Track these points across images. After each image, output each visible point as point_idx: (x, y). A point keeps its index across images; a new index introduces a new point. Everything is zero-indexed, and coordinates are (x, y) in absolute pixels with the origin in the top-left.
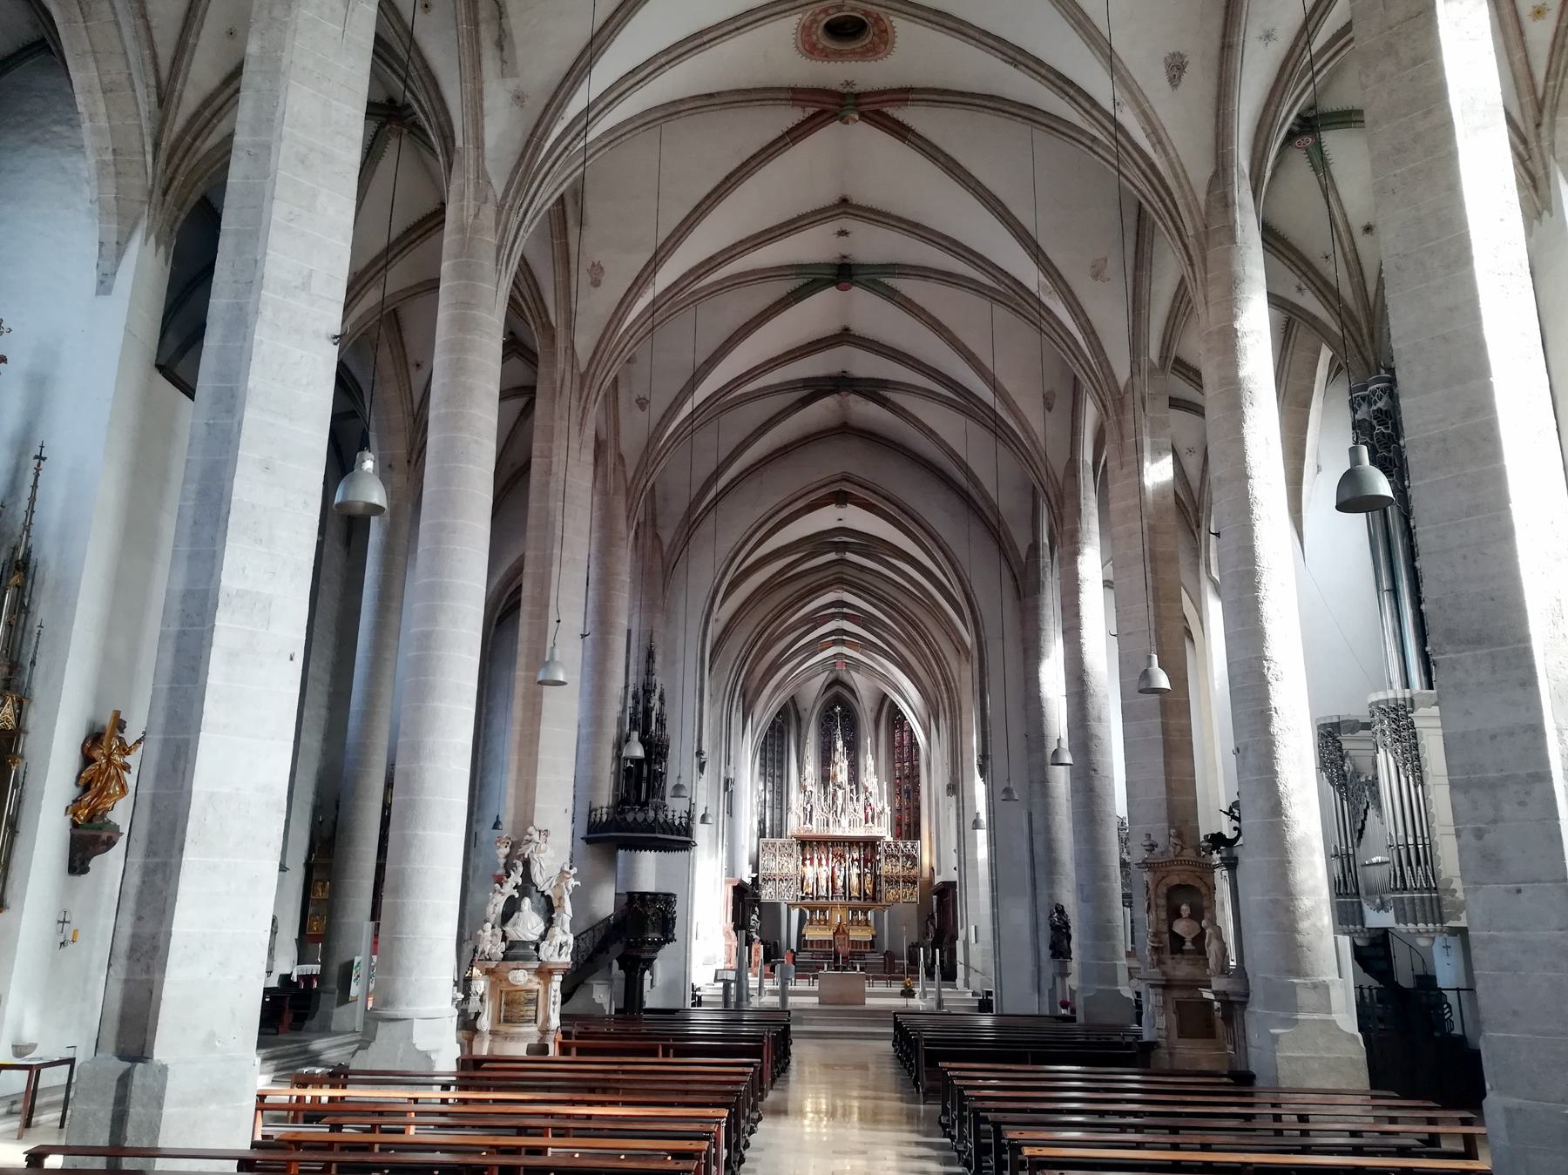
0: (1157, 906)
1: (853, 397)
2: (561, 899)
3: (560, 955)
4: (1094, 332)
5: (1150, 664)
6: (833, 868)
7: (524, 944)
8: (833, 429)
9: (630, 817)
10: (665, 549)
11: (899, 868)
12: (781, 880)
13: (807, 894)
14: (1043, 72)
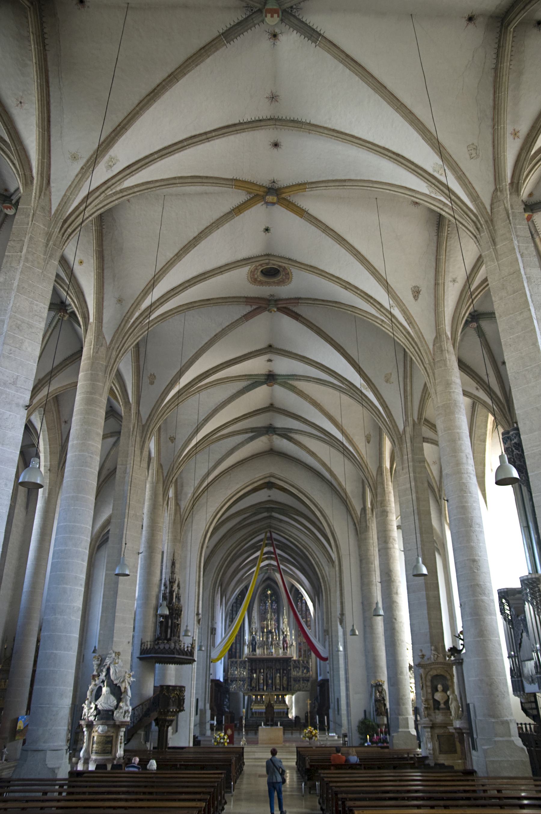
0: (426, 686)
1: (275, 437)
3: (124, 717)
4: (387, 407)
6: (267, 674)
8: (265, 452)
9: (162, 646)
10: (182, 511)
11: (300, 673)
12: (240, 680)
13: (253, 687)
14: (359, 292)
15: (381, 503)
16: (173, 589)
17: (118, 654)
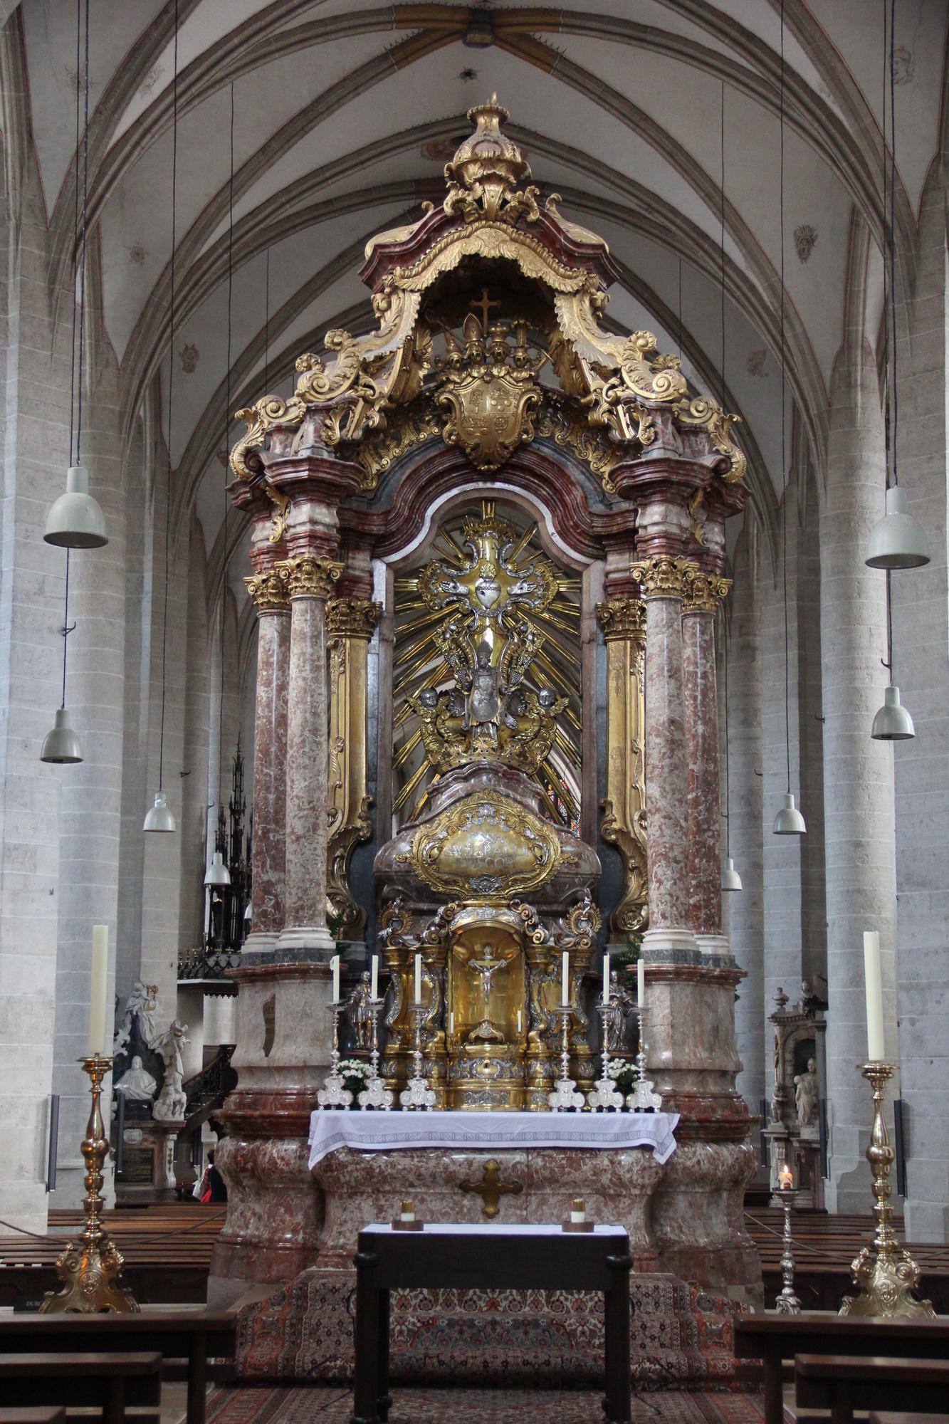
0: (784, 1061)
2: (173, 1057)
3: (173, 1113)
4: (750, 433)
5: (788, 806)
7: (139, 1103)
10: (240, 608)
15: (741, 627)
16: (241, 827)
17: (154, 990)
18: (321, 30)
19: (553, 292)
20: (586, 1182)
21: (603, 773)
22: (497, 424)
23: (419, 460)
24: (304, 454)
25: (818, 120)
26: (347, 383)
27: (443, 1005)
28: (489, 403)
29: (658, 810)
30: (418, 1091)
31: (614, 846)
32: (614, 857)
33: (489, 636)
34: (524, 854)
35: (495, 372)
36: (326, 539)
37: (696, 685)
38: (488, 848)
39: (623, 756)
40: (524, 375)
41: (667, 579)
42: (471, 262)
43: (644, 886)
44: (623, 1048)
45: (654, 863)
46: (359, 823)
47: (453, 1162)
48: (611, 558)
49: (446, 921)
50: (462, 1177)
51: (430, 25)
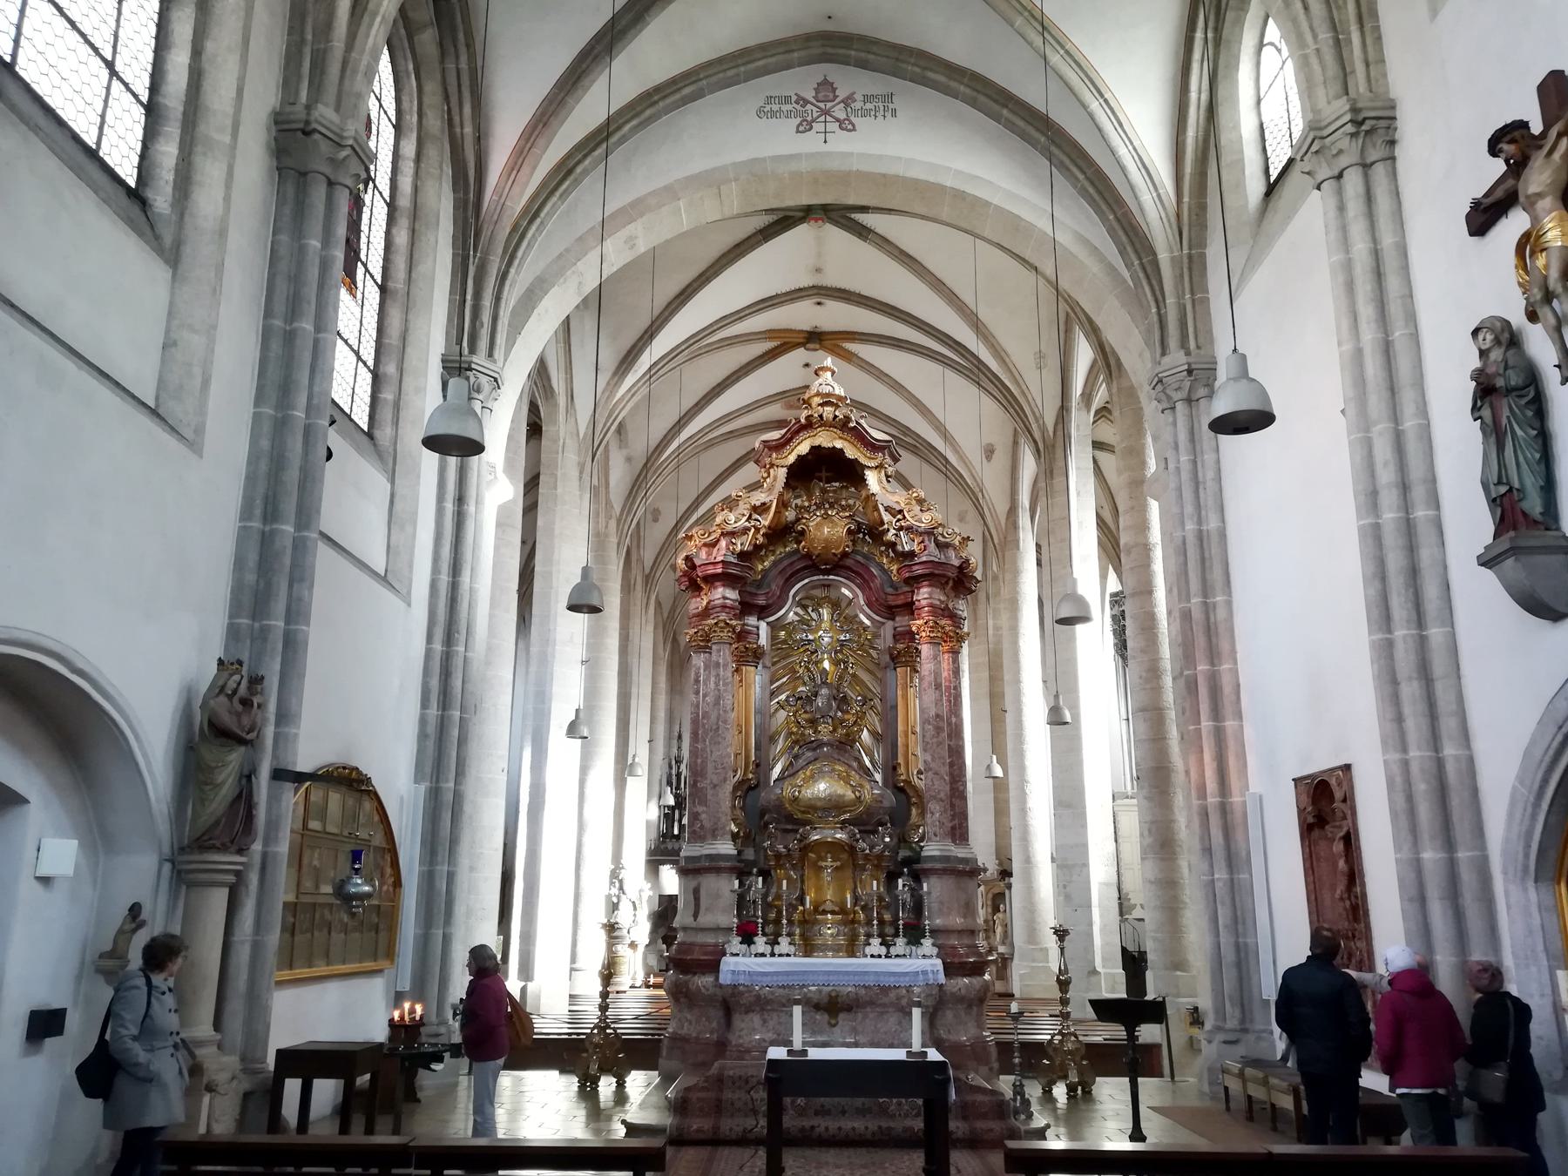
9: (670, 847)
18: (729, 342)
19: (864, 467)
20: (892, 1005)
21: (895, 745)
22: (828, 543)
23: (786, 563)
24: (720, 559)
25: (997, 387)
26: (745, 518)
27: (802, 889)
28: (826, 530)
29: (930, 769)
30: (784, 945)
31: (902, 790)
32: (903, 797)
33: (826, 665)
34: (850, 795)
35: (830, 513)
36: (732, 608)
37: (950, 694)
38: (828, 792)
39: (906, 736)
40: (847, 514)
41: (933, 632)
42: (815, 450)
43: (922, 814)
44: (912, 917)
45: (928, 802)
46: (750, 776)
47: (810, 991)
48: (897, 619)
49: (804, 837)
50: (816, 1001)
51: (786, 340)
